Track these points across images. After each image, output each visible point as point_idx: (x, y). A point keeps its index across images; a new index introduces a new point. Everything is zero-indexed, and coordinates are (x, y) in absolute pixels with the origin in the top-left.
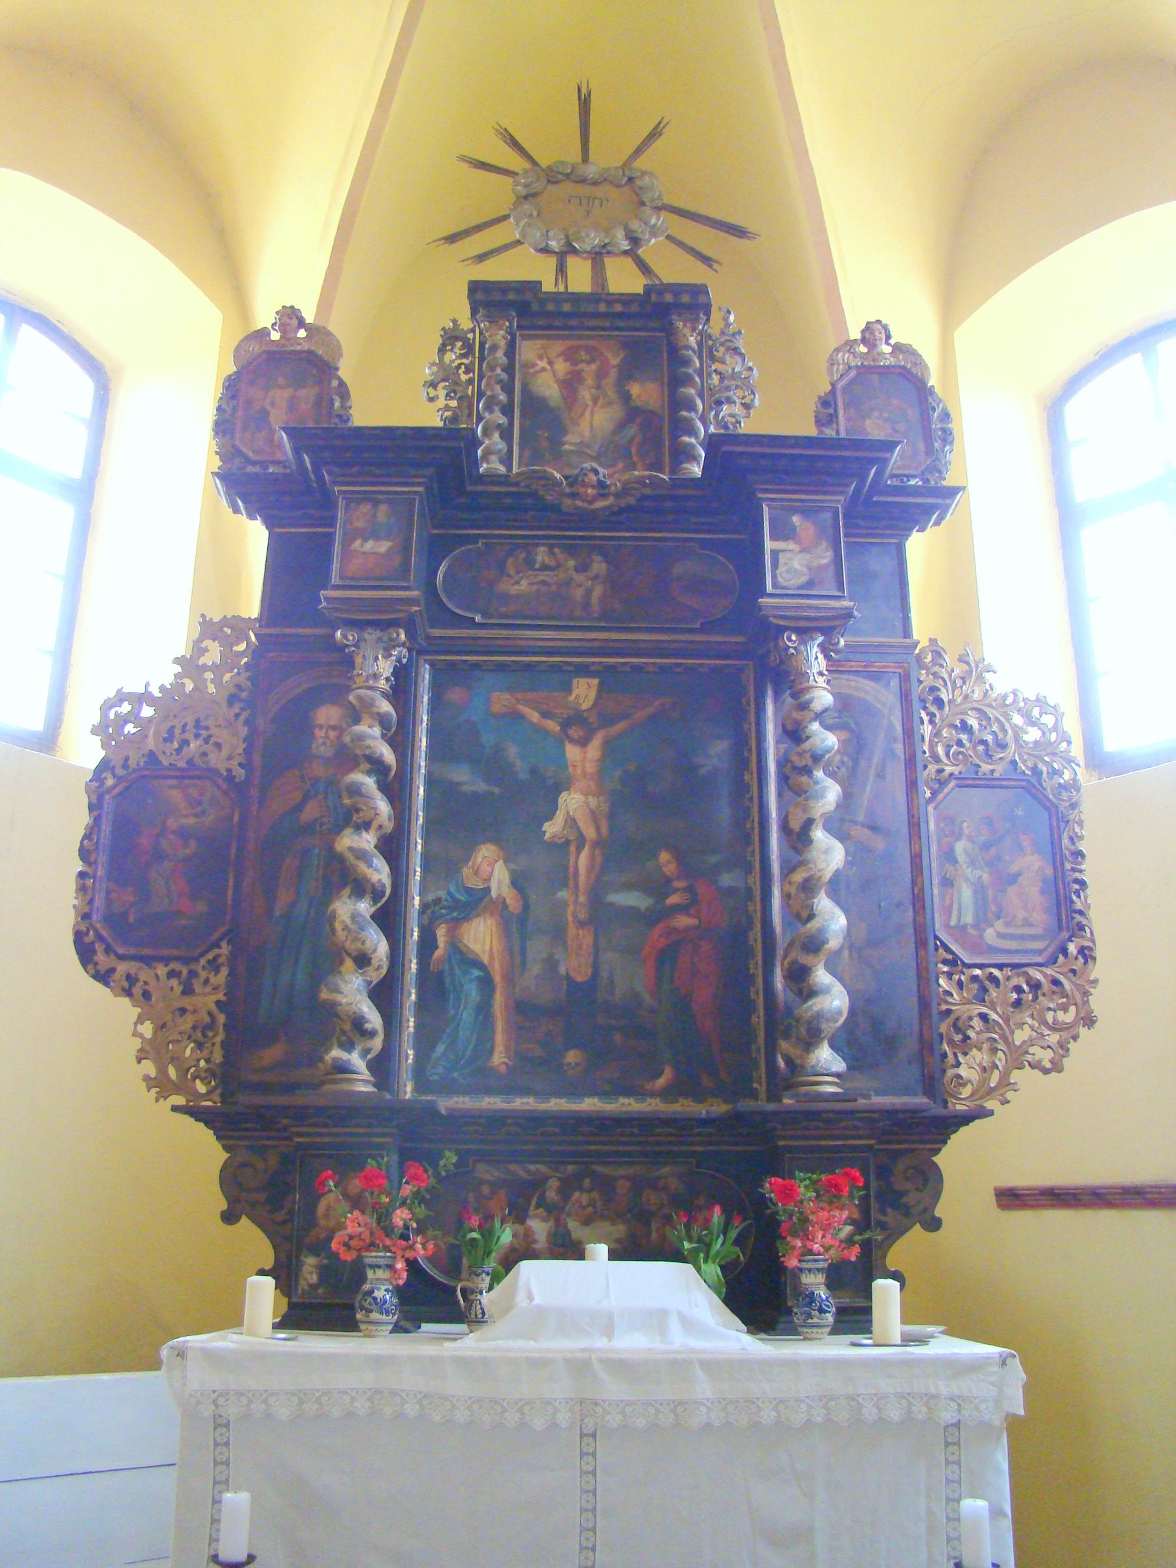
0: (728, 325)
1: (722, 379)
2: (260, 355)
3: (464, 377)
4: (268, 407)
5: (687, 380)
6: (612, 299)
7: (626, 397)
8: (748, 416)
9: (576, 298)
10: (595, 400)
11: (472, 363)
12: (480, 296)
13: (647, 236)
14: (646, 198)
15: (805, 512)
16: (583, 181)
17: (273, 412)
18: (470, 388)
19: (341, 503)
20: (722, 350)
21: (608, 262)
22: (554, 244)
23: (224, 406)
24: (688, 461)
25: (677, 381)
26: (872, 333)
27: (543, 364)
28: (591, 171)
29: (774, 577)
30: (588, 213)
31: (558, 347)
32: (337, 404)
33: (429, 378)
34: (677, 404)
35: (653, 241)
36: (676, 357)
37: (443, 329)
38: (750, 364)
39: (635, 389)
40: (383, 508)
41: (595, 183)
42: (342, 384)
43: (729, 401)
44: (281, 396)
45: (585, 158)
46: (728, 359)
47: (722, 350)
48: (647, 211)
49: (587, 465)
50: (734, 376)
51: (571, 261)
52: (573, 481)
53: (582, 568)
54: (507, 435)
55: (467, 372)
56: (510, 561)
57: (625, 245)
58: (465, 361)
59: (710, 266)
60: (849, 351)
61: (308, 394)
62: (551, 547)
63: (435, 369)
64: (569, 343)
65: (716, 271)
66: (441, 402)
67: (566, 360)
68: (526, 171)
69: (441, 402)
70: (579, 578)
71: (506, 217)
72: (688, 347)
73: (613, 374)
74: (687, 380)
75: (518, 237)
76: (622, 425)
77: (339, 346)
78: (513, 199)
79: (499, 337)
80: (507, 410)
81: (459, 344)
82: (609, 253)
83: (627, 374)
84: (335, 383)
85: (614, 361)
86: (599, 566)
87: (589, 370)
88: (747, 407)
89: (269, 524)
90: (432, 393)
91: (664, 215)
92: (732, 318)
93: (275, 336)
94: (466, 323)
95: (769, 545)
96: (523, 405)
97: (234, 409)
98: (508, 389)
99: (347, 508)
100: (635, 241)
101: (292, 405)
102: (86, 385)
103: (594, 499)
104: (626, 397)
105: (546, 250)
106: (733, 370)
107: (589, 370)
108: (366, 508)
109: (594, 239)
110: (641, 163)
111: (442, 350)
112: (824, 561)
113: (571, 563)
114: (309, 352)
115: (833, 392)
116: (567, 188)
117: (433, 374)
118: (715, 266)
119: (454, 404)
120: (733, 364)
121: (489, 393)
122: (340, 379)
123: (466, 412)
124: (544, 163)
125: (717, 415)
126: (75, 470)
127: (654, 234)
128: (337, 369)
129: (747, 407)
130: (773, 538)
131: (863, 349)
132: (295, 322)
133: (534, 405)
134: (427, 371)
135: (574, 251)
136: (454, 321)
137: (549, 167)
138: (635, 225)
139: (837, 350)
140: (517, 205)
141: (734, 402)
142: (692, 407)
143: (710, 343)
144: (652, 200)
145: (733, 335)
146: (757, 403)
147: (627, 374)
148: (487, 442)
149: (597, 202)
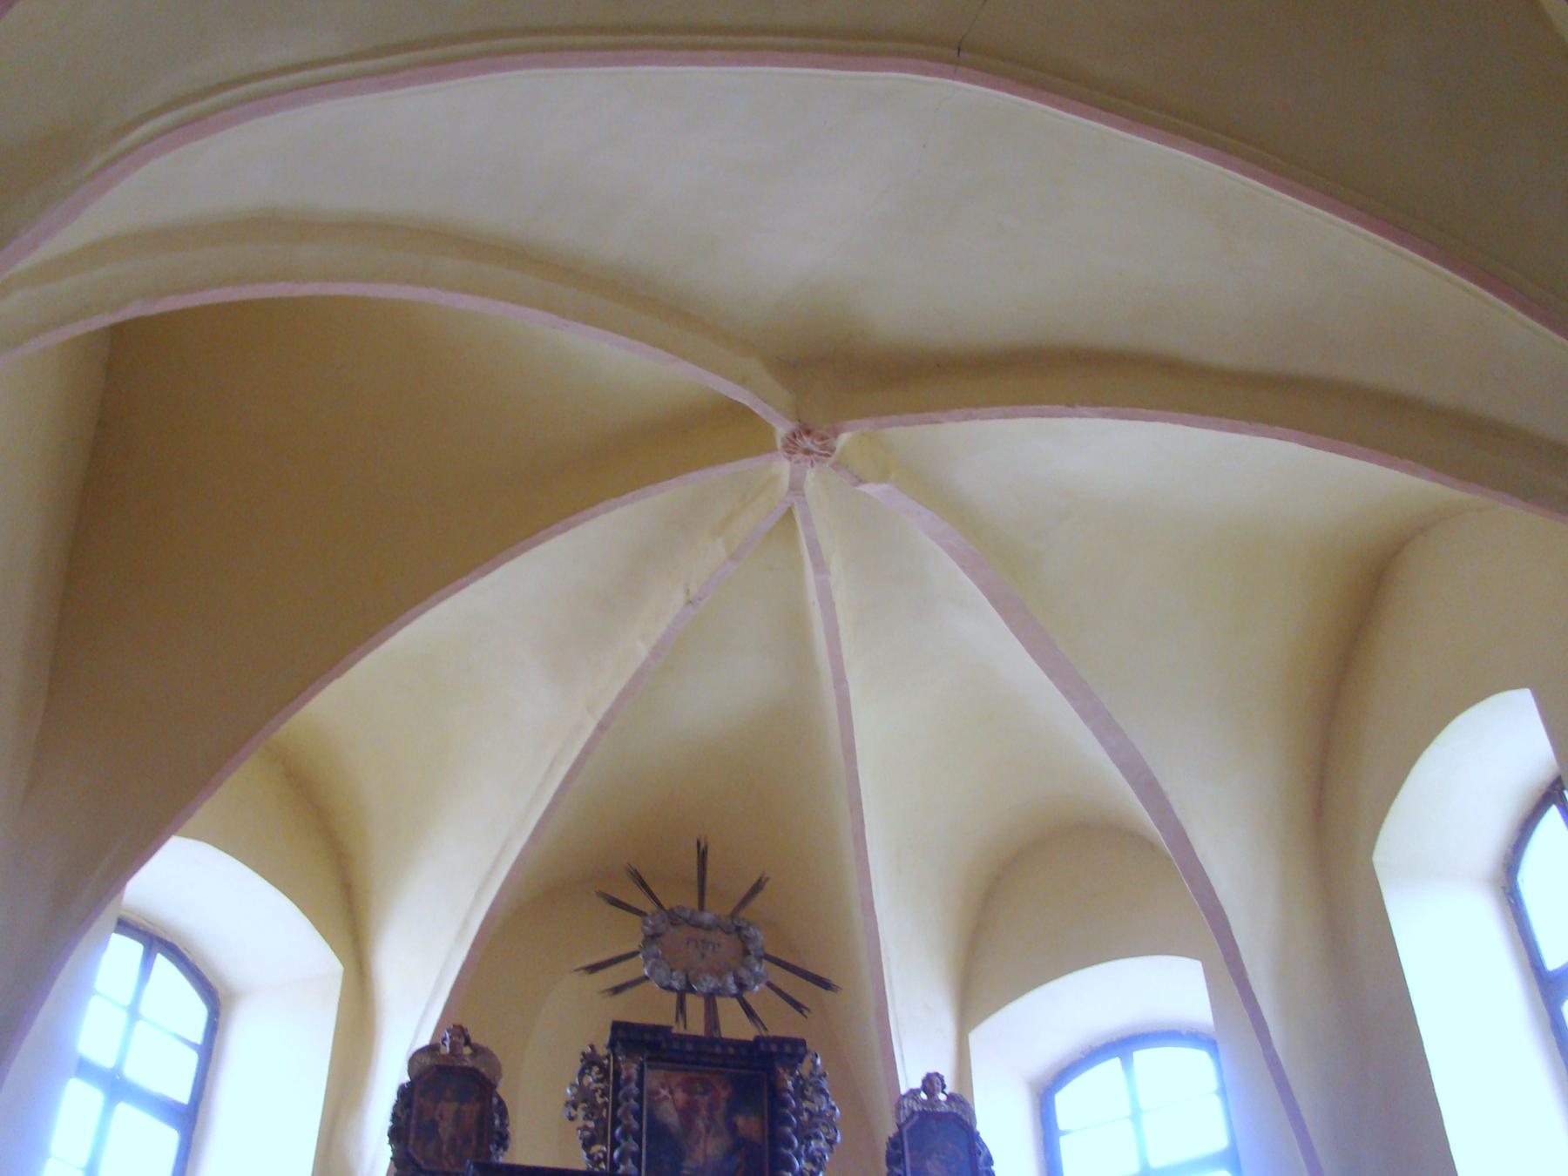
4: (437, 1118)
5: (787, 1121)
7: (733, 1128)
8: (831, 1151)
9: (696, 1039)
10: (708, 1129)
11: (607, 1088)
13: (753, 983)
14: (751, 947)
16: (699, 926)
20: (811, 1089)
21: (719, 1001)
22: (676, 984)
23: (399, 1114)
27: (664, 1092)
28: (707, 917)
30: (703, 955)
31: (677, 1078)
32: (497, 1122)
34: (776, 1140)
37: (583, 1054)
38: (833, 1103)
39: (740, 1121)
41: (709, 928)
42: (501, 1102)
43: (817, 1137)
44: (449, 1108)
45: (702, 908)
46: (816, 1099)
50: (821, 1114)
54: (637, 1159)
57: (733, 989)
58: (600, 1085)
59: (801, 1012)
60: (913, 1099)
61: (471, 1110)
63: (575, 1090)
65: (806, 1017)
67: (684, 1091)
69: (580, 1122)
71: (634, 954)
73: (723, 1105)
75: (646, 973)
77: (499, 1066)
78: (642, 937)
81: (596, 1069)
82: (720, 995)
84: (495, 1101)
87: (703, 1101)
88: (831, 1142)
90: (573, 1113)
91: (765, 963)
92: (819, 1061)
96: (649, 1129)
97: (409, 1117)
100: (741, 986)
104: (733, 1128)
105: (669, 988)
106: (820, 1108)
107: (703, 1101)
109: (709, 983)
111: (582, 1074)
115: (900, 1134)
117: (574, 1095)
118: (806, 1012)
119: (591, 1124)
121: (625, 1122)
124: (667, 907)
127: (757, 981)
128: (496, 1087)
129: (831, 1142)
131: (923, 1096)
132: (463, 1041)
133: (658, 1131)
134: (568, 1091)
135: (692, 991)
137: (672, 911)
138: (743, 973)
140: (644, 942)
141: (821, 1138)
142: (790, 1144)
145: (820, 1077)
146: (839, 1138)
149: (711, 947)
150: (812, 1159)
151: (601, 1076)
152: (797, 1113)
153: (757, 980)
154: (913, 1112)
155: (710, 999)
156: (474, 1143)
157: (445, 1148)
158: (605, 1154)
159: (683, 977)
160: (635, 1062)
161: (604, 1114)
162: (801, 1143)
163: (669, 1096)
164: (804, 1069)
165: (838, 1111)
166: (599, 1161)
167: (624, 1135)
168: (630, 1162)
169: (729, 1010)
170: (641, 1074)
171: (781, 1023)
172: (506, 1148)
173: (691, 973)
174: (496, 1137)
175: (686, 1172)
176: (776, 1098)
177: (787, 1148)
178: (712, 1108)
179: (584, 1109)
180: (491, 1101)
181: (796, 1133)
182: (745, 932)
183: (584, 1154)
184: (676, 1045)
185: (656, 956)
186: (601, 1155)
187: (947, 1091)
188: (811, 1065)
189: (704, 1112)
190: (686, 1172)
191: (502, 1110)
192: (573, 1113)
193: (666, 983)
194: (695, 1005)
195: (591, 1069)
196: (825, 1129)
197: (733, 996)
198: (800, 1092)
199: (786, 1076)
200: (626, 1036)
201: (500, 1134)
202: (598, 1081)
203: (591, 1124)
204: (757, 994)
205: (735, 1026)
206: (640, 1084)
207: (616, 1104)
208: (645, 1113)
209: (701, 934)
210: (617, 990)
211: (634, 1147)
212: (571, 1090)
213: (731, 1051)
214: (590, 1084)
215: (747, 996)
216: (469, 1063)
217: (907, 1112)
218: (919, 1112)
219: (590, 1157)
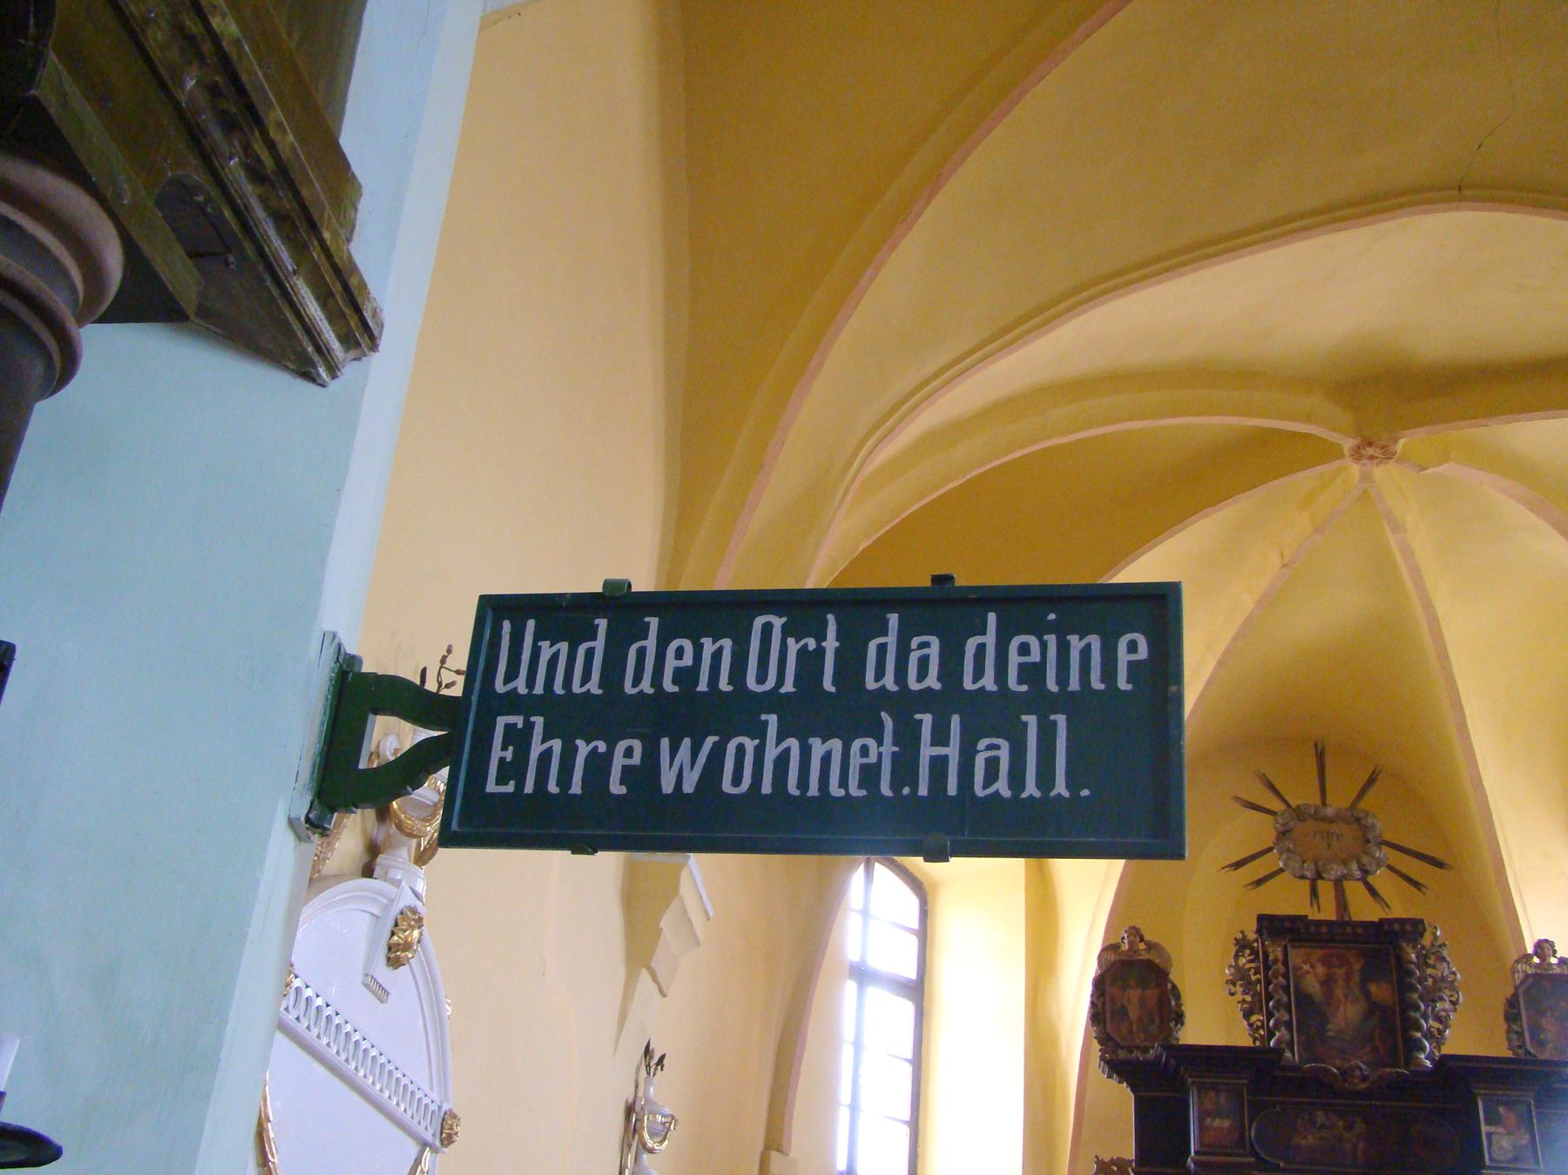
2: (1115, 963)
3: (1253, 978)
5: (1412, 988)
7: (1367, 996)
8: (1455, 1011)
9: (1329, 923)
10: (1345, 996)
12: (1265, 923)
13: (1374, 868)
14: (1370, 836)
16: (1324, 819)
17: (1130, 1008)
18: (1259, 986)
20: (1433, 957)
21: (1347, 885)
22: (1307, 874)
23: (1096, 1002)
24: (1418, 1050)
26: (1542, 949)
27: (1306, 967)
28: (1329, 811)
29: (1490, 1153)
30: (1329, 845)
31: (1318, 953)
32: (1173, 1003)
34: (1406, 1006)
35: (1378, 872)
36: (1401, 962)
37: (1236, 939)
38: (1454, 969)
39: (1373, 988)
40: (1223, 1095)
41: (1331, 821)
42: (1174, 987)
43: (1442, 999)
44: (1134, 994)
45: (1324, 804)
46: (1438, 966)
47: (1433, 957)
49: (1353, 1063)
50: (1443, 979)
51: (1320, 882)
52: (1344, 1073)
53: (1349, 1127)
54: (1288, 1025)
56: (1299, 1121)
57: (1358, 874)
58: (1253, 965)
59: (1419, 889)
60: (1526, 963)
61: (1152, 993)
64: (1325, 951)
65: (1425, 894)
66: (1239, 997)
67: (1323, 965)
68: (1283, 813)
69: (1239, 997)
70: (1348, 1135)
71: (1270, 850)
72: (1412, 962)
73: (1357, 978)
74: (1412, 988)
75: (1281, 865)
77: (1169, 956)
78: (1274, 834)
81: (1248, 952)
82: (1346, 879)
83: (1368, 976)
84: (1169, 986)
85: (1357, 966)
86: (1360, 1126)
87: (1340, 972)
88: (1454, 1003)
92: (1438, 933)
93: (1125, 947)
94: (1252, 936)
95: (1484, 1128)
96: (1297, 1000)
97: (1104, 1004)
98: (1286, 989)
100: (1366, 872)
104: (1367, 996)
105: (1302, 877)
106: (1442, 974)
107: (1340, 972)
109: (1336, 870)
110: (1363, 805)
111: (1236, 957)
112: (1524, 1142)
113: (1340, 1124)
114: (1149, 962)
115: (1515, 995)
116: (1310, 826)
117: (1231, 975)
118: (1423, 889)
119: (1249, 998)
120: (1443, 969)
122: (1172, 982)
123: (1258, 1006)
124: (1293, 803)
125: (1433, 1009)
127: (1378, 866)
128: (1168, 974)
129: (1454, 1003)
130: (1489, 1122)
131: (1536, 960)
132: (1138, 939)
133: (1304, 1000)
134: (1227, 971)
135: (1322, 878)
136: (1242, 932)
137: (1298, 806)
138: (1365, 859)
139: (1518, 961)
140: (1278, 839)
141: (1445, 1000)
142: (1417, 1008)
143: (1424, 952)
144: (1375, 837)
145: (1440, 946)
146: (1461, 999)
147: (1368, 976)
148: (1277, 1034)
149: (1335, 838)
150: (1438, 1019)
151: (1252, 957)
152: (1421, 980)
153: (1379, 864)
154: (1527, 976)
155: (1338, 884)
156: (1157, 1021)
157: (1134, 1026)
158: (1262, 1022)
159: (1312, 867)
160: (1279, 946)
161: (1258, 989)
162: (1427, 1006)
163: (1311, 970)
164: (1426, 940)
165: (1458, 976)
166: (1258, 1028)
167: (1276, 1007)
168: (1283, 1029)
169: (1355, 891)
170: (1286, 955)
171: (1399, 905)
172: (1182, 1024)
173: (1320, 863)
174: (1174, 1016)
177: (1415, 1012)
178: (1348, 977)
179: (1241, 985)
180: (1166, 985)
181: (1421, 998)
182: (1364, 822)
183: (1245, 1023)
184: (1313, 929)
185: (1288, 851)
186: (1259, 1024)
187: (1558, 955)
188: (1432, 937)
189: (1341, 982)
190: (1330, 1034)
191: (1178, 996)
192: (1233, 990)
193: (1300, 874)
194: (1326, 889)
195: (1243, 952)
197: (1359, 879)
198: (1423, 961)
199: (1409, 949)
200: (1270, 925)
201: (1177, 1013)
202: (1251, 961)
203: (1249, 998)
204: (1380, 878)
205: (1364, 910)
206: (1285, 963)
207: (1268, 982)
209: (1325, 826)
210: (1259, 882)
211: (1286, 1018)
212: (1229, 970)
213: (1360, 931)
214: (1244, 965)
215: (1370, 879)
216: (1145, 956)
219: (1251, 1025)
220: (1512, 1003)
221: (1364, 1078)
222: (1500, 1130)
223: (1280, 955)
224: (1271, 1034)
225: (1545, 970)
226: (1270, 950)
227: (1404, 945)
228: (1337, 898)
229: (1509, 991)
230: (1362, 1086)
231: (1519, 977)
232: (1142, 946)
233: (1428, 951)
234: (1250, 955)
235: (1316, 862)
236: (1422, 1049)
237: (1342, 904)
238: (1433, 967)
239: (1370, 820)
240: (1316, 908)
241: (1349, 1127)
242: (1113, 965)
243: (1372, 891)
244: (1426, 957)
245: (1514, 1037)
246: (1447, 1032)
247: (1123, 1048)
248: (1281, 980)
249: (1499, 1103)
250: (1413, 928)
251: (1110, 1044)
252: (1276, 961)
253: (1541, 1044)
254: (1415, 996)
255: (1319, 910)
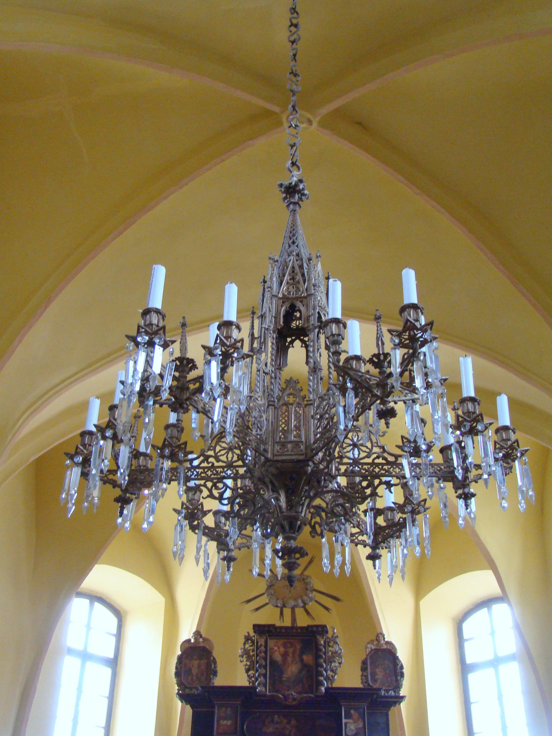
0: (334, 633)
1: (332, 654)
3: (251, 654)
5: (321, 657)
6: (297, 628)
9: (286, 628)
10: (292, 661)
13: (309, 602)
14: (308, 587)
15: (356, 709)
17: (193, 669)
19: (216, 707)
20: (332, 642)
21: (297, 610)
22: (279, 605)
23: (178, 666)
25: (317, 657)
26: (379, 638)
27: (276, 648)
29: (345, 732)
30: (290, 592)
31: (281, 642)
32: (213, 667)
33: (241, 654)
34: (319, 665)
39: (305, 657)
40: (229, 709)
42: (214, 659)
43: (335, 662)
44: (196, 663)
46: (335, 646)
47: (332, 642)
48: (308, 592)
51: (284, 609)
55: (252, 652)
57: (301, 604)
58: (252, 648)
59: (329, 611)
62: (279, 715)
63: (242, 650)
66: (244, 663)
67: (283, 647)
70: (288, 726)
72: (321, 645)
73: (298, 652)
74: (321, 657)
76: (300, 671)
77: (213, 644)
78: (266, 587)
79: (262, 641)
80: (265, 667)
81: (250, 641)
82: (297, 607)
83: (302, 652)
84: (212, 658)
85: (298, 647)
86: (293, 722)
87: (291, 650)
88: (340, 663)
89: (192, 707)
90: (242, 659)
91: (314, 593)
92: (335, 631)
93: (193, 641)
96: (270, 662)
97: (181, 667)
98: (265, 659)
99: (218, 708)
100: (305, 604)
101: (199, 666)
102: (114, 620)
103: (292, 702)
104: (302, 660)
105: (277, 606)
107: (291, 650)
108: (223, 709)
109: (292, 603)
110: (306, 573)
111: (245, 644)
113: (285, 721)
115: (366, 659)
118: (330, 611)
121: (260, 662)
123: (253, 666)
126: (112, 656)
127: (311, 601)
129: (340, 663)
130: (346, 718)
132: (199, 637)
133: (273, 663)
135: (286, 607)
136: (248, 633)
138: (305, 598)
142: (322, 666)
143: (328, 640)
147: (302, 652)
148: (259, 679)
150: (332, 671)
151: (252, 644)
152: (325, 653)
153: (311, 599)
155: (293, 609)
156: (205, 675)
157: (194, 678)
158: (254, 675)
159: (282, 601)
164: (330, 635)
165: (343, 650)
167: (260, 667)
168: (262, 677)
169: (299, 612)
172: (216, 676)
174: (213, 672)
175: (284, 679)
176: (318, 650)
177: (321, 668)
178: (294, 653)
179: (246, 657)
181: (325, 662)
182: (306, 581)
183: (246, 675)
184: (278, 630)
185: (271, 594)
186: (252, 675)
188: (332, 633)
189: (291, 655)
190: (284, 679)
191: (215, 662)
192: (242, 659)
194: (287, 612)
195: (248, 641)
196: (337, 658)
197: (302, 607)
199: (321, 639)
200: (259, 629)
203: (248, 663)
204: (311, 606)
205: (303, 621)
206: (266, 646)
207: (257, 655)
208: (268, 657)
210: (257, 609)
211: (264, 671)
213: (299, 630)
214: (248, 648)
215: (307, 607)
216: (202, 645)
217: (369, 650)
218: (374, 649)
219: (248, 676)
220: (364, 663)
221: (294, 699)
222: (351, 721)
223: (263, 643)
224: (257, 680)
225: (380, 647)
226: (259, 640)
227: (318, 637)
228: (292, 616)
229: (364, 657)
230: (295, 703)
231: (368, 650)
232: (201, 640)
233: (330, 639)
234: (251, 643)
235: (283, 599)
236: (323, 685)
237: (294, 619)
238: (332, 647)
239: (309, 580)
240: (282, 620)
241: (289, 722)
242: (187, 649)
243: (308, 613)
244: (329, 642)
245: (364, 678)
246: (336, 677)
247: (188, 688)
248: (263, 654)
249: (351, 708)
250: (322, 629)
251: (183, 686)
252: (261, 646)
253: (375, 681)
254: (322, 661)
255: (283, 622)
